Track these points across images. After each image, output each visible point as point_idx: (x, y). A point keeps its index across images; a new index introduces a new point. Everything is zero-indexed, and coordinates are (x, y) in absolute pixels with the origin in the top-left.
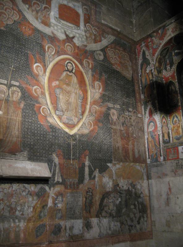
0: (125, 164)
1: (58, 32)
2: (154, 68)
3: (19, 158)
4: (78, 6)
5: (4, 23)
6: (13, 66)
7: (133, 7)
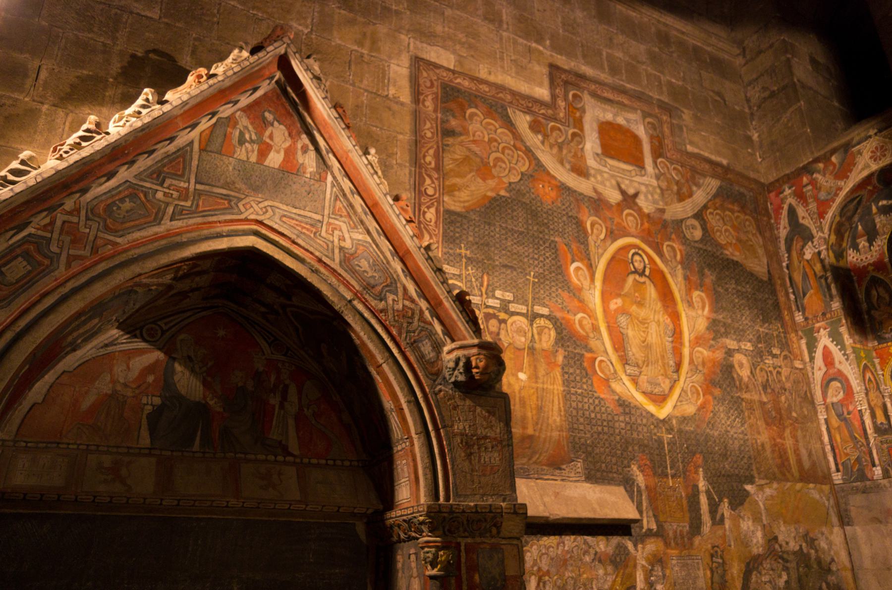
0: (785, 486)
2: (825, 247)
3: (568, 477)
4: (634, 120)
5: (505, 180)
6: (532, 274)
7: (748, 100)
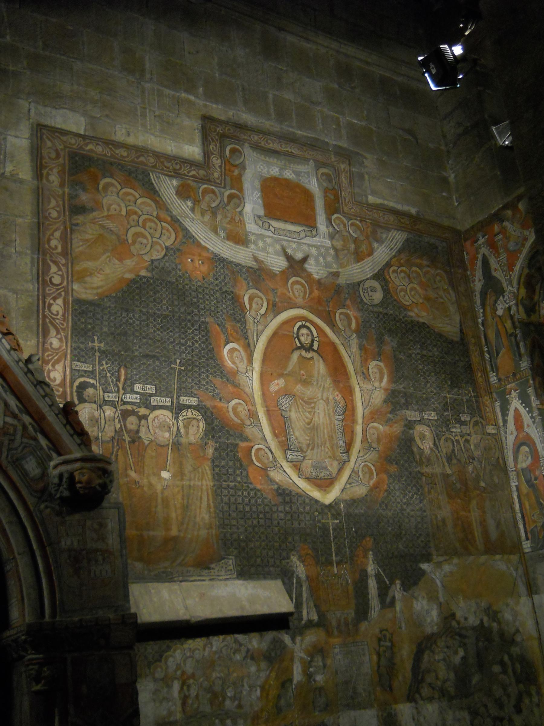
1: (268, 253)
2: (514, 302)
3: (219, 576)
4: (305, 172)
6: (178, 361)
7: (444, 136)
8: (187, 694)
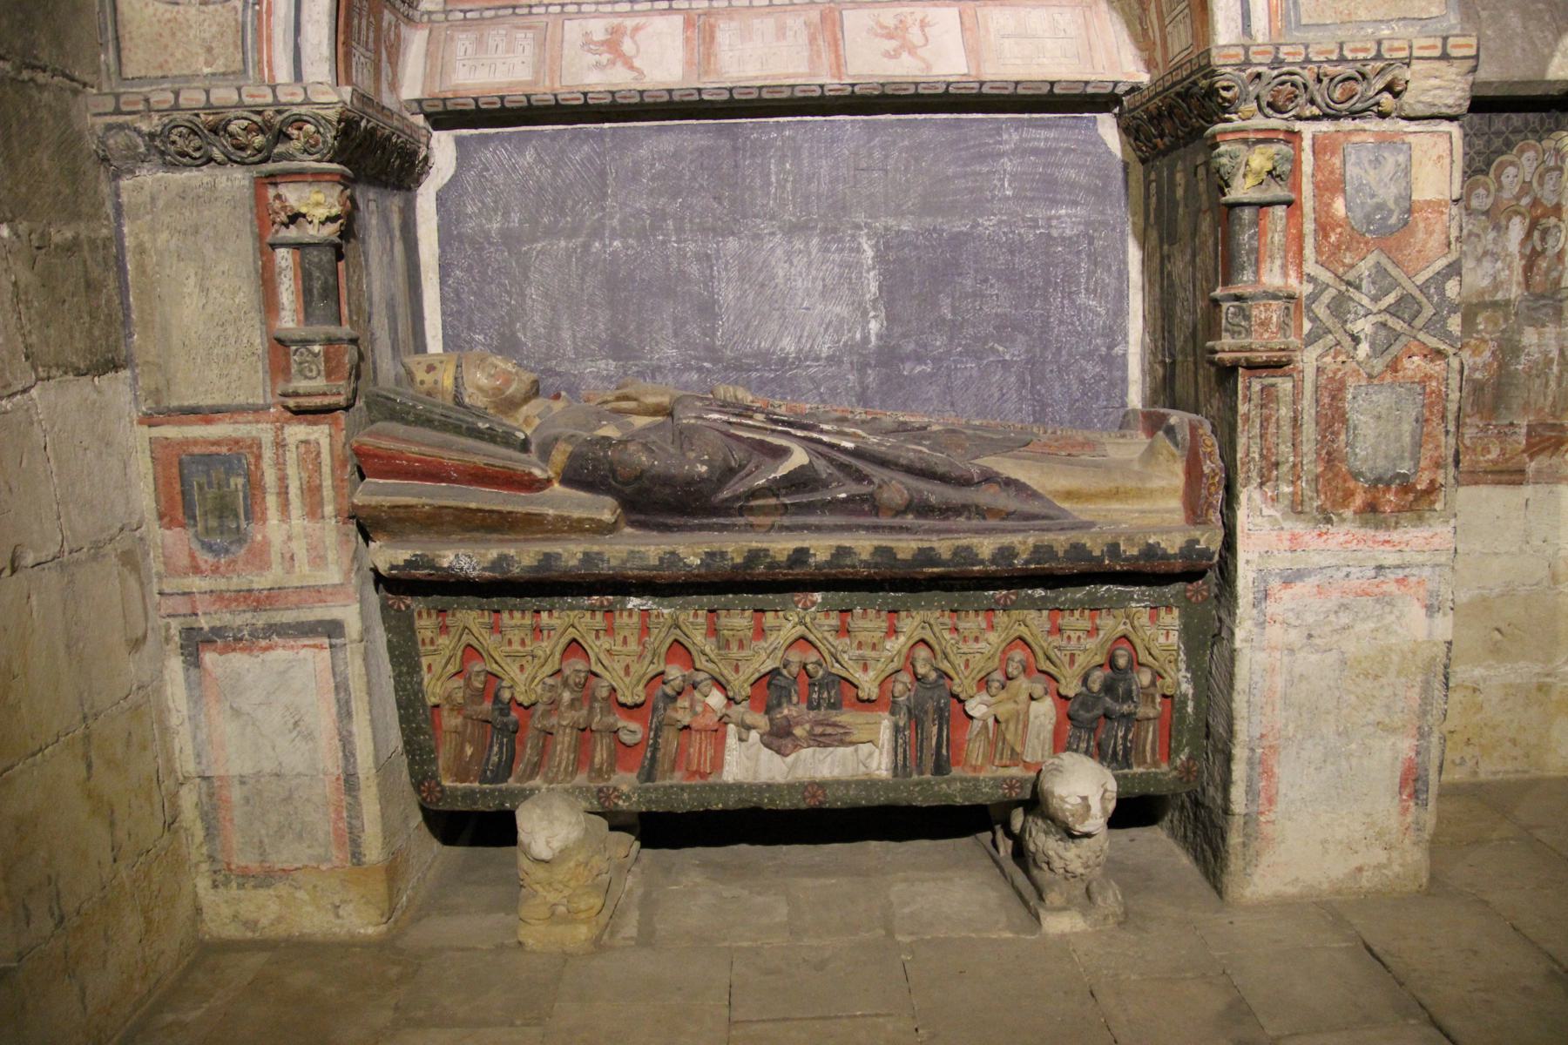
8: (1539, 248)
